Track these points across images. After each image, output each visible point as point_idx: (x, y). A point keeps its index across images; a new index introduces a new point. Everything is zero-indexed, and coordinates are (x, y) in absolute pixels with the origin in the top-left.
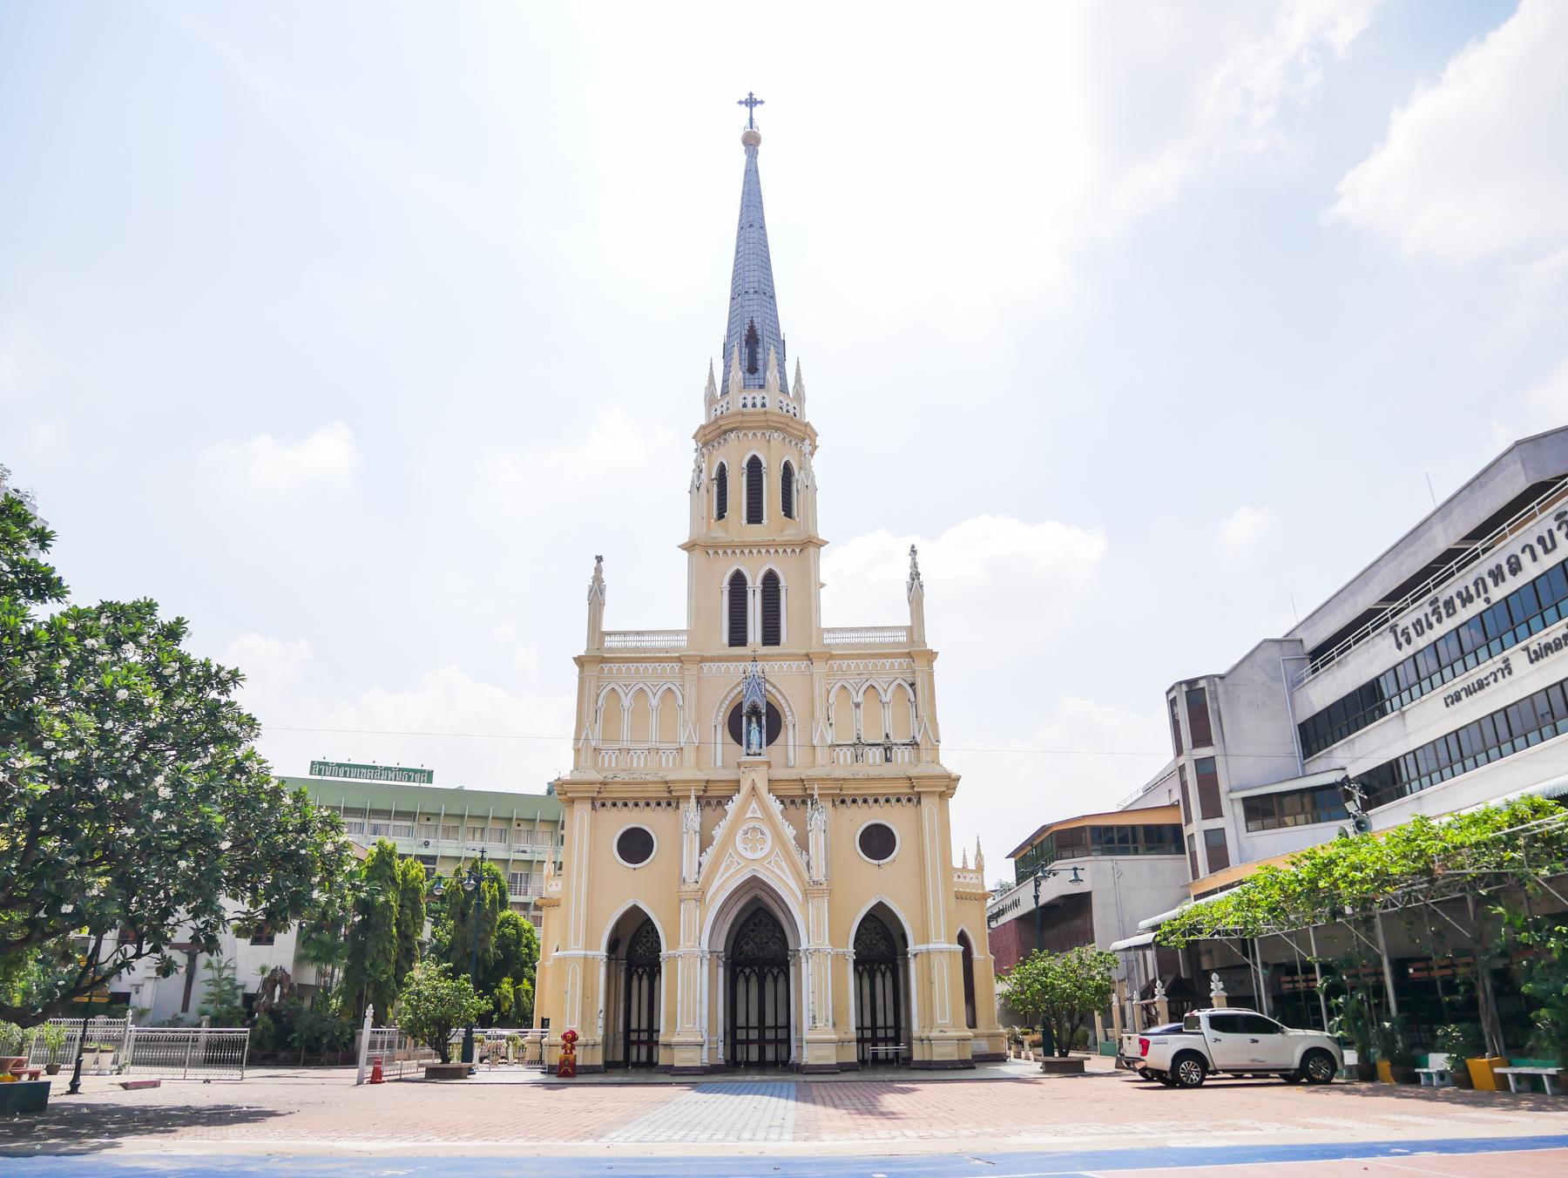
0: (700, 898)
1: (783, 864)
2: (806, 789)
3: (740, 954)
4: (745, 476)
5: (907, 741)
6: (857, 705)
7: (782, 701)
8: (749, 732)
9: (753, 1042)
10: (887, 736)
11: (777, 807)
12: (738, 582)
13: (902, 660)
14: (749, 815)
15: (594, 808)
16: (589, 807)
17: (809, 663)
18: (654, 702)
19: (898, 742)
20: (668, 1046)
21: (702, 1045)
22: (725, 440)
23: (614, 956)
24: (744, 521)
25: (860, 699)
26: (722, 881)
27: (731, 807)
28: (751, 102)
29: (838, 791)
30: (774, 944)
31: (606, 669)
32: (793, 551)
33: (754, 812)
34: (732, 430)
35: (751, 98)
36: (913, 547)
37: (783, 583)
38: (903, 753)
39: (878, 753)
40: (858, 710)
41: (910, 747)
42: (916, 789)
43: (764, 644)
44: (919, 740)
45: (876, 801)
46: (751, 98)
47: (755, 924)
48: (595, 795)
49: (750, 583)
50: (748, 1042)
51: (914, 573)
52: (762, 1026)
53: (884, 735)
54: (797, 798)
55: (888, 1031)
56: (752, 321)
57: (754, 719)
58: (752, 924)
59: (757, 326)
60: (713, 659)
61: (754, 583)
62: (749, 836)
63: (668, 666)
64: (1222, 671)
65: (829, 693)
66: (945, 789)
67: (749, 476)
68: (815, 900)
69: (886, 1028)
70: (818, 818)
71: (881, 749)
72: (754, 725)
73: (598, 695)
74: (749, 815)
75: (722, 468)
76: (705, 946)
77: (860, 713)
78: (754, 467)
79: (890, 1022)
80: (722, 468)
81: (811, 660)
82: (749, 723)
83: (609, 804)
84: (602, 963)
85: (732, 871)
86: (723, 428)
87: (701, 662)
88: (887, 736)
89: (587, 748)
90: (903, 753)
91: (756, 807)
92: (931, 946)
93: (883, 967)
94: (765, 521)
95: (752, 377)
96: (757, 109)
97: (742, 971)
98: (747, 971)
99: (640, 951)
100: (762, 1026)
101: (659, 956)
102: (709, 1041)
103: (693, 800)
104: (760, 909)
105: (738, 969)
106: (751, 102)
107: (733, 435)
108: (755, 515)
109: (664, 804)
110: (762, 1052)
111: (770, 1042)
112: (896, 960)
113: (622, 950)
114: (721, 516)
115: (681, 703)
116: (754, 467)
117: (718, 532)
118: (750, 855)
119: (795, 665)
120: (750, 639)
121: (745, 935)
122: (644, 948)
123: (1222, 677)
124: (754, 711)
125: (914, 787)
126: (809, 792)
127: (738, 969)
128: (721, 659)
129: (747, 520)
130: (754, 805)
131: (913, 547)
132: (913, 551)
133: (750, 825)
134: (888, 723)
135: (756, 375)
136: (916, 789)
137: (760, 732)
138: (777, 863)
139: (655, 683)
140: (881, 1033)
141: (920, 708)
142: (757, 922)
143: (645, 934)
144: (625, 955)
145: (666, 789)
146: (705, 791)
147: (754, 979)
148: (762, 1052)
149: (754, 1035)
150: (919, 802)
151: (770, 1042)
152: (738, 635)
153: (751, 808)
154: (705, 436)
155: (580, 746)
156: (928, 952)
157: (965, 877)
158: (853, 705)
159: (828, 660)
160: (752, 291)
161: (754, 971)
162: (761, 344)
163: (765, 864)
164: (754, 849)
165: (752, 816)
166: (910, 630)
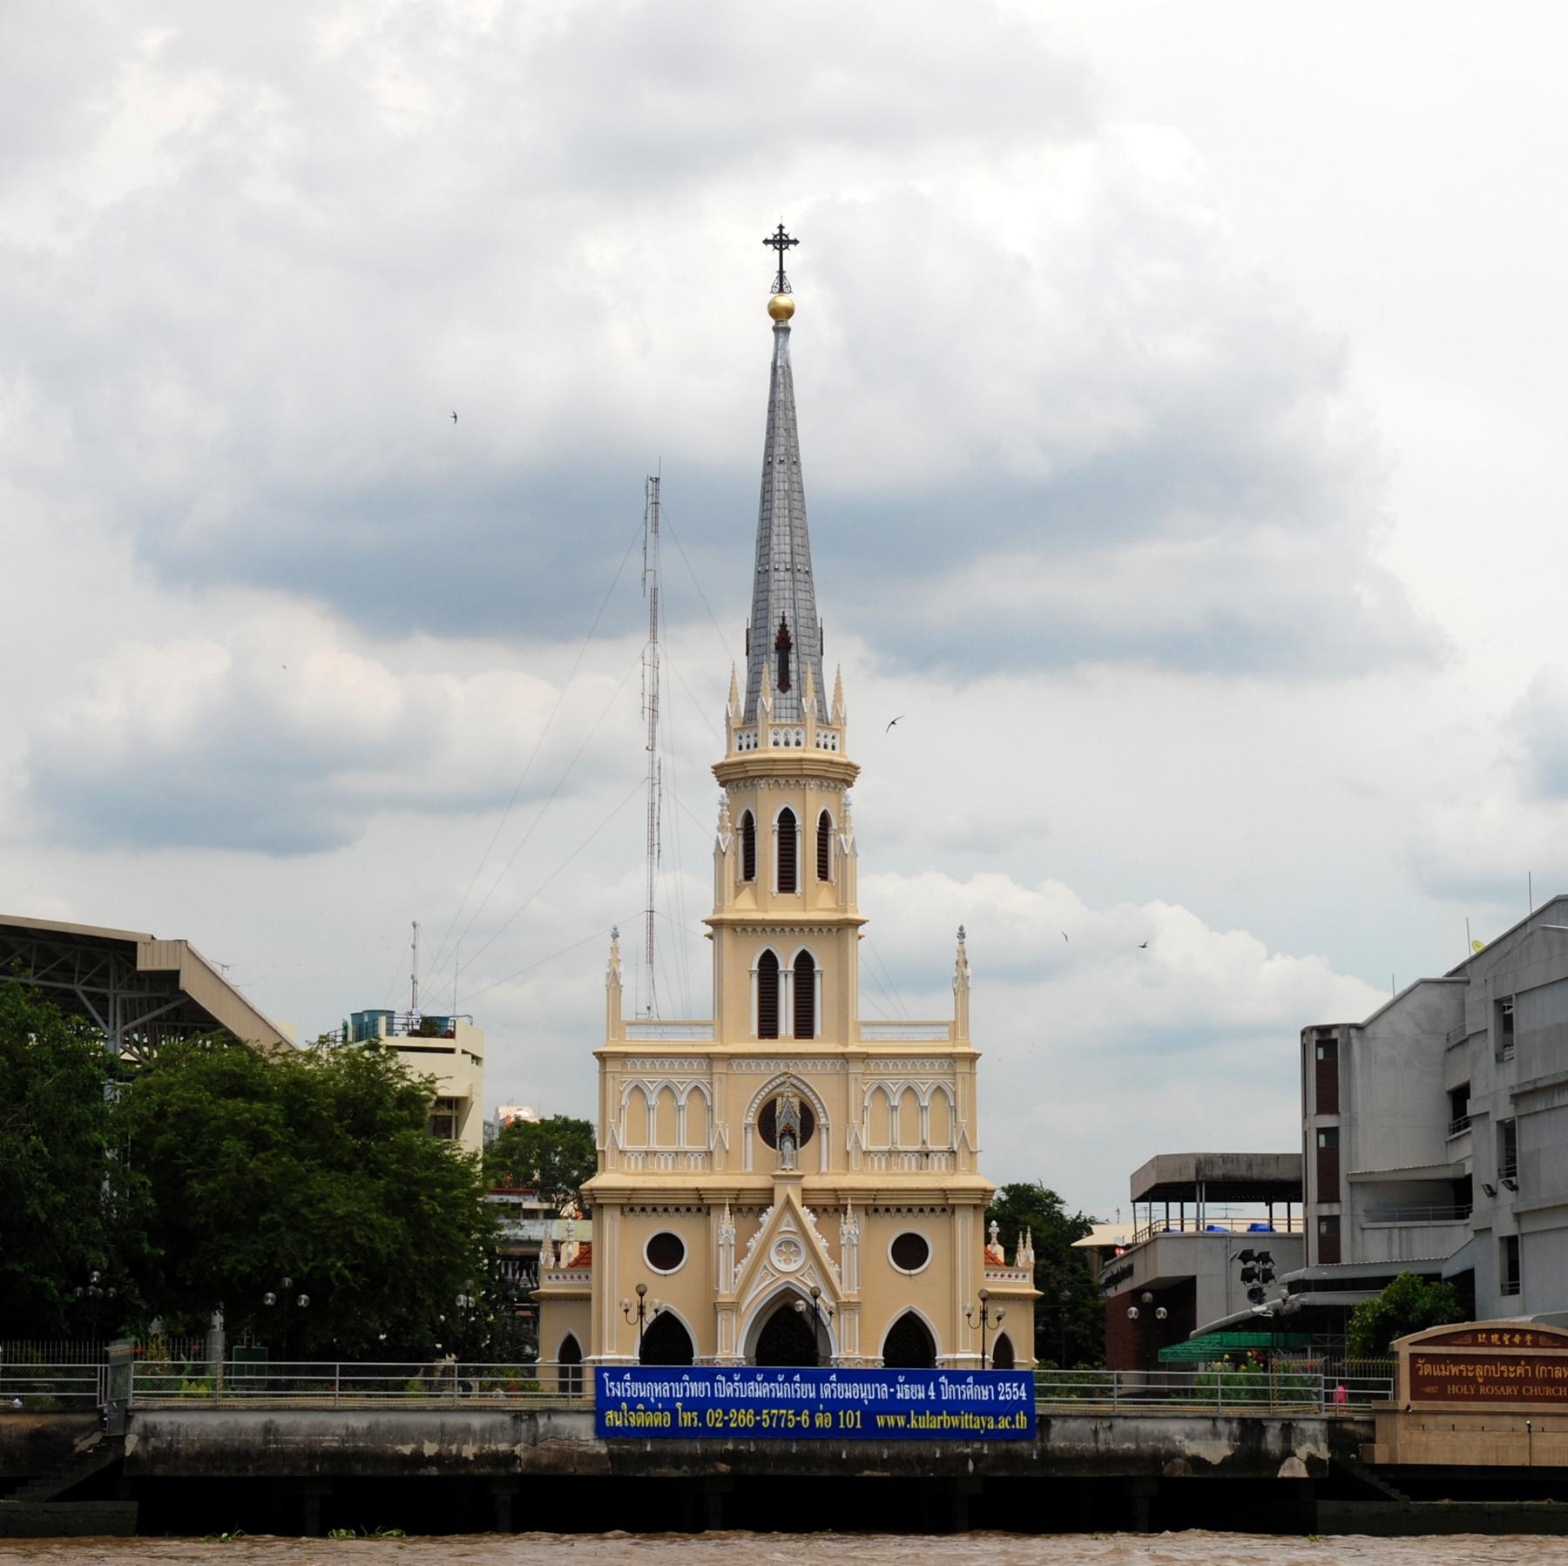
0: (734, 1307)
2: (839, 1199)
4: (776, 833)
10: (924, 1143)
11: (808, 1218)
12: (768, 963)
16: (619, 1213)
19: (935, 1148)
22: (752, 784)
24: (775, 888)
26: (757, 1291)
27: (766, 1219)
28: (781, 242)
29: (871, 1202)
34: (761, 777)
35: (781, 234)
36: (961, 929)
44: (955, 1149)
46: (781, 234)
49: (781, 968)
51: (961, 961)
54: (830, 1206)
56: (784, 618)
59: (791, 630)
62: (783, 1248)
64: (1360, 1019)
68: (847, 1312)
70: (851, 1226)
77: (897, 1117)
78: (787, 819)
83: (638, 1209)
87: (729, 1059)
88: (924, 1143)
90: (940, 1159)
92: (958, 1356)
94: (799, 889)
95: (783, 696)
96: (790, 254)
103: (727, 1208)
106: (781, 242)
108: (787, 882)
109: (694, 1209)
116: (787, 819)
117: (745, 907)
123: (1359, 1028)
126: (842, 1202)
129: (780, 883)
130: (788, 1217)
131: (961, 929)
132: (962, 935)
134: (929, 1133)
135: (788, 693)
136: (950, 1202)
150: (953, 1213)
152: (768, 1028)
153: (785, 1221)
157: (1017, 1276)
160: (782, 567)
162: (793, 650)
163: (798, 1276)
164: (788, 1261)
166: (953, 1026)
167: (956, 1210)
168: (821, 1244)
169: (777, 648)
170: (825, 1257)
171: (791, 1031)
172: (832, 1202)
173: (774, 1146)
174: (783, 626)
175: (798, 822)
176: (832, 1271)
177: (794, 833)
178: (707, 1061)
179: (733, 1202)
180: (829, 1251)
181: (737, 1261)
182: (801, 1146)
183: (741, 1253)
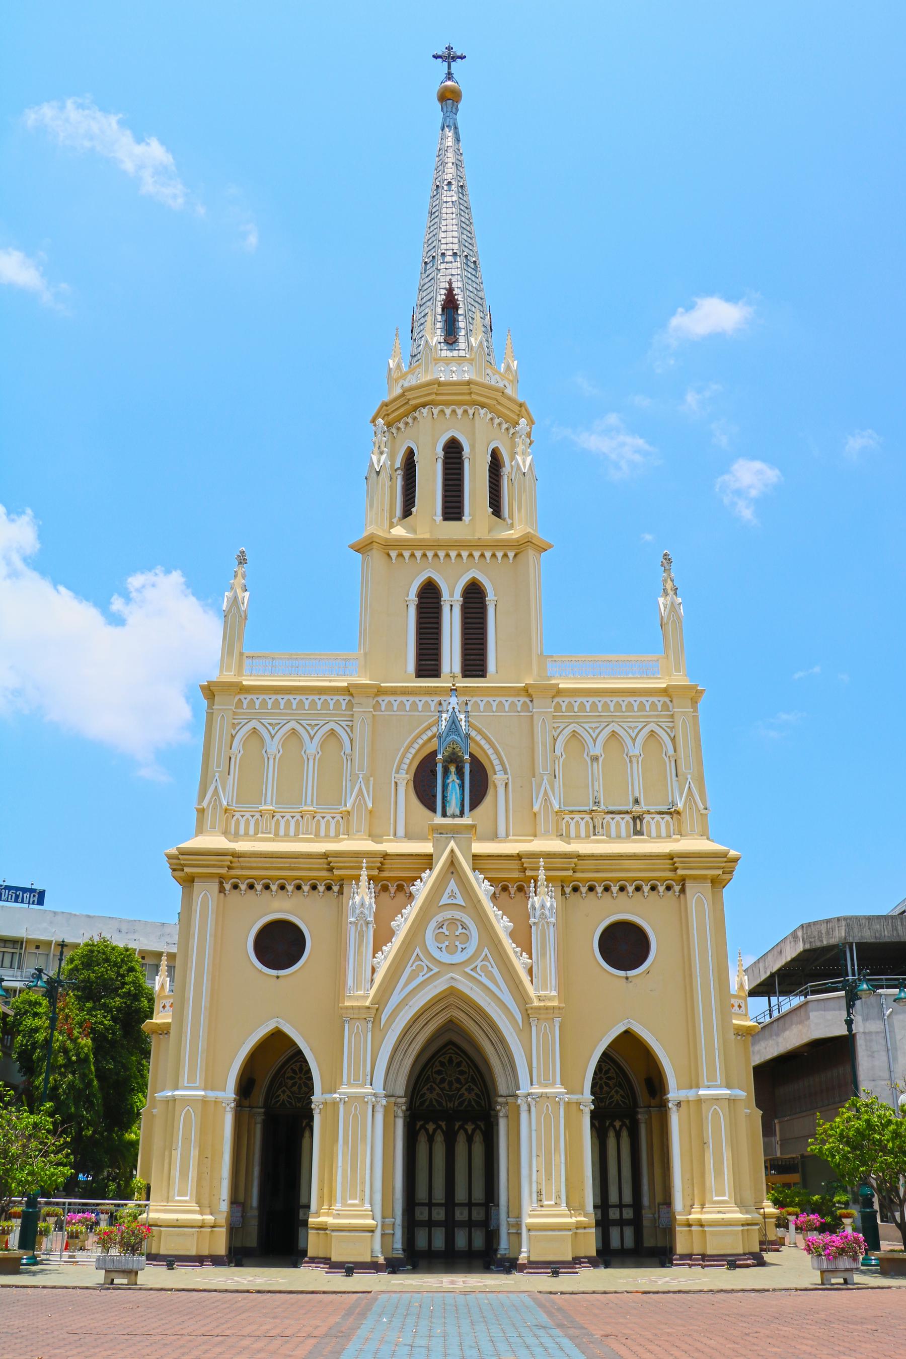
1: (495, 972)
2: (525, 869)
3: (422, 1104)
5: (664, 808)
6: (595, 759)
7: (490, 752)
8: (445, 787)
9: (438, 1224)
10: (636, 801)
13: (655, 699)
14: (445, 900)
15: (222, 890)
16: (215, 887)
17: (527, 700)
18: (312, 748)
19: (653, 809)
20: (323, 1228)
21: (372, 1231)
22: (415, 419)
23: (246, 1103)
24: (439, 517)
25: (597, 750)
30: (470, 1090)
31: (245, 702)
32: (505, 555)
33: (452, 896)
34: (424, 405)
37: (490, 598)
38: (658, 825)
39: (623, 825)
40: (595, 764)
41: (668, 817)
42: (680, 872)
43: (465, 675)
44: (680, 806)
45: (622, 889)
47: (442, 1064)
48: (224, 871)
49: (445, 596)
50: (430, 1224)
52: (450, 1203)
53: (631, 799)
55: (625, 1211)
56: (450, 283)
57: (453, 769)
58: (437, 1063)
60: (394, 692)
61: (452, 595)
62: (444, 930)
63: (332, 700)
65: (555, 740)
66: (720, 872)
67: (445, 463)
68: (543, 1024)
69: (621, 1206)
71: (628, 818)
72: (453, 777)
73: (233, 737)
74: (445, 900)
75: (410, 454)
76: (379, 1089)
77: (598, 768)
78: (453, 450)
79: (628, 1198)
80: (410, 454)
81: (530, 696)
82: (446, 772)
84: (228, 1109)
85: (420, 979)
86: (412, 402)
88: (636, 801)
89: (214, 808)
90: (658, 825)
91: (456, 890)
94: (466, 518)
97: (423, 1127)
98: (431, 1127)
99: (284, 1097)
100: (450, 1203)
101: (311, 1102)
102: (383, 1226)
104: (451, 1043)
105: (419, 1124)
106: (450, 57)
107: (425, 411)
110: (450, 1239)
111: (461, 1224)
112: (637, 1113)
113: (259, 1095)
114: (407, 512)
115: (348, 751)
116: (453, 450)
118: (445, 958)
119: (507, 701)
120: (445, 668)
121: (428, 1078)
122: (288, 1093)
124: (454, 759)
125: (676, 869)
128: (405, 692)
130: (452, 885)
133: (448, 914)
136: (680, 872)
137: (462, 786)
138: (485, 968)
139: (313, 723)
140: (614, 1214)
141: (682, 764)
142: (446, 1061)
143: (289, 1074)
144: (261, 1104)
145: (325, 866)
146: (380, 869)
147: (439, 1138)
148: (450, 1239)
149: (439, 1214)
150: (683, 890)
151: (461, 1224)
153: (448, 890)
154: (388, 415)
155: (205, 804)
156: (700, 1101)
158: (588, 760)
159: (553, 697)
160: (450, 253)
161: (439, 1127)
163: (468, 970)
164: (452, 950)
165: (450, 901)
167: (689, 886)
168: (502, 924)
169: (443, 310)
170: (509, 946)
171: (457, 668)
172: (516, 875)
173: (434, 810)
174: (450, 291)
175: (466, 452)
176: (520, 963)
177: (461, 463)
178: (348, 698)
179: (375, 872)
180: (512, 935)
181: (377, 949)
182: (471, 810)
183: (382, 937)
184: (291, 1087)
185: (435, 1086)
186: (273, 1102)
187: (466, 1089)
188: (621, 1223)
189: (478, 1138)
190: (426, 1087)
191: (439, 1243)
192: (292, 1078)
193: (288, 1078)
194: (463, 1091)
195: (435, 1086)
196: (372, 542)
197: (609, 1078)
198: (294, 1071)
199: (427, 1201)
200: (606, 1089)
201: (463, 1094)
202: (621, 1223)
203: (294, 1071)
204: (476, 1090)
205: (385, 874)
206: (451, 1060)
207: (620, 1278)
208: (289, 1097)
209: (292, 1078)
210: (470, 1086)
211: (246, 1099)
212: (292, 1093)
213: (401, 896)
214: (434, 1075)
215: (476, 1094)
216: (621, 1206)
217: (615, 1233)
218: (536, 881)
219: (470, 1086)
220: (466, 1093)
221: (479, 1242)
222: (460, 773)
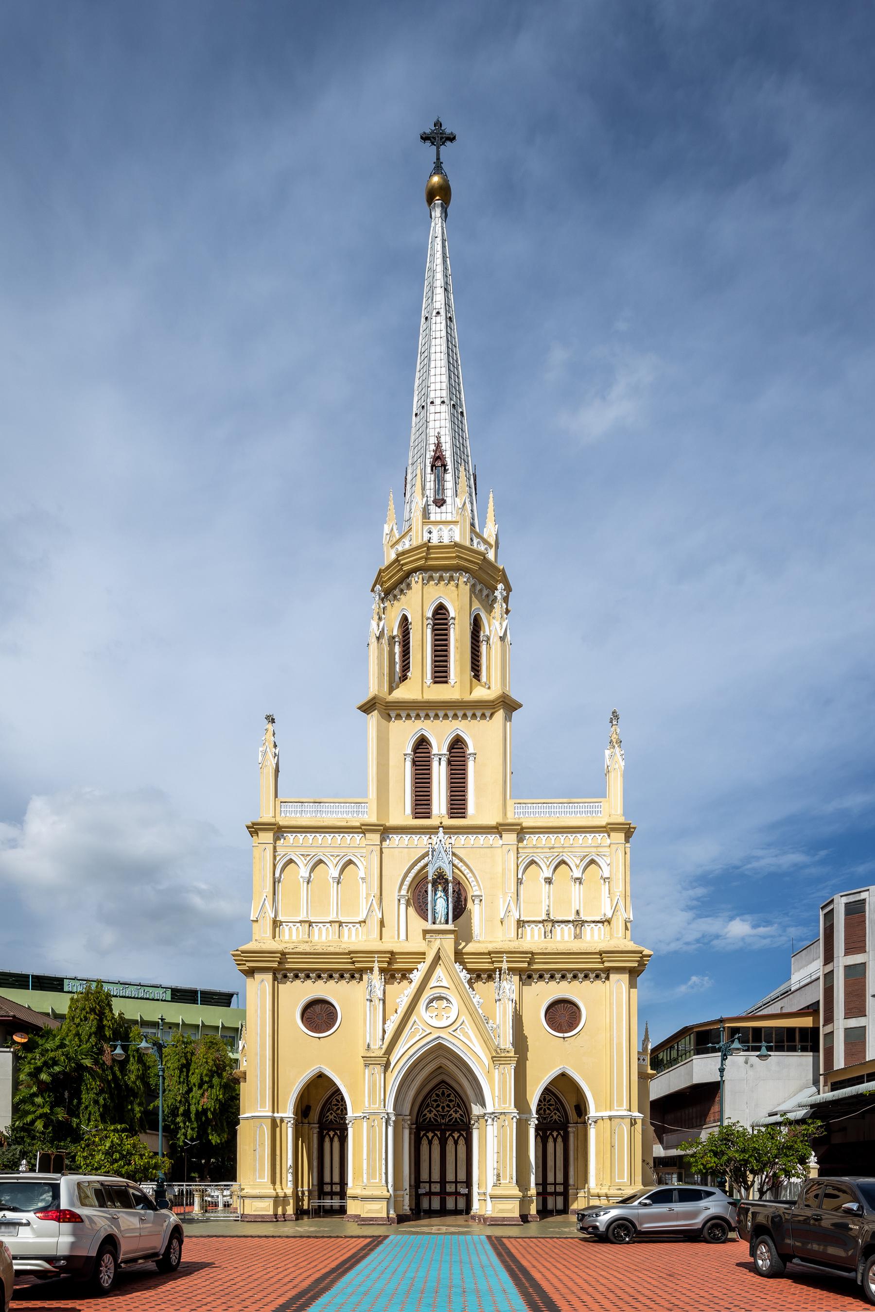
9: (435, 1194)
30: (456, 1112)
47: (437, 1095)
50: (430, 1194)
52: (443, 1181)
58: (434, 1095)
93: (555, 1134)
98: (430, 1135)
99: (331, 1117)
100: (443, 1181)
105: (422, 1133)
110: (443, 1202)
111: (450, 1194)
127: (422, 1133)
147: (436, 1142)
148: (443, 1202)
149: (436, 1188)
151: (450, 1194)
161: (436, 1135)
184: (336, 1111)
185: (432, 1109)
186: (324, 1120)
187: (454, 1111)
188: (556, 1194)
189: (462, 1142)
190: (427, 1110)
191: (436, 1204)
192: (336, 1105)
193: (333, 1105)
194: (451, 1112)
195: (432, 1109)
196: (375, 703)
197: (551, 1105)
198: (338, 1101)
199: (428, 1180)
200: (548, 1111)
201: (452, 1114)
202: (556, 1194)
203: (338, 1101)
204: (461, 1112)
205: (396, 966)
206: (443, 1093)
207: (551, 1228)
208: (335, 1117)
209: (336, 1105)
210: (456, 1109)
211: (305, 1118)
212: (336, 1114)
213: (405, 982)
214: (433, 1103)
215: (460, 1114)
216: (555, 1184)
217: (550, 1200)
218: (500, 971)
219: (456, 1109)
220: (454, 1114)
221: (462, 1205)
222: (445, 891)
